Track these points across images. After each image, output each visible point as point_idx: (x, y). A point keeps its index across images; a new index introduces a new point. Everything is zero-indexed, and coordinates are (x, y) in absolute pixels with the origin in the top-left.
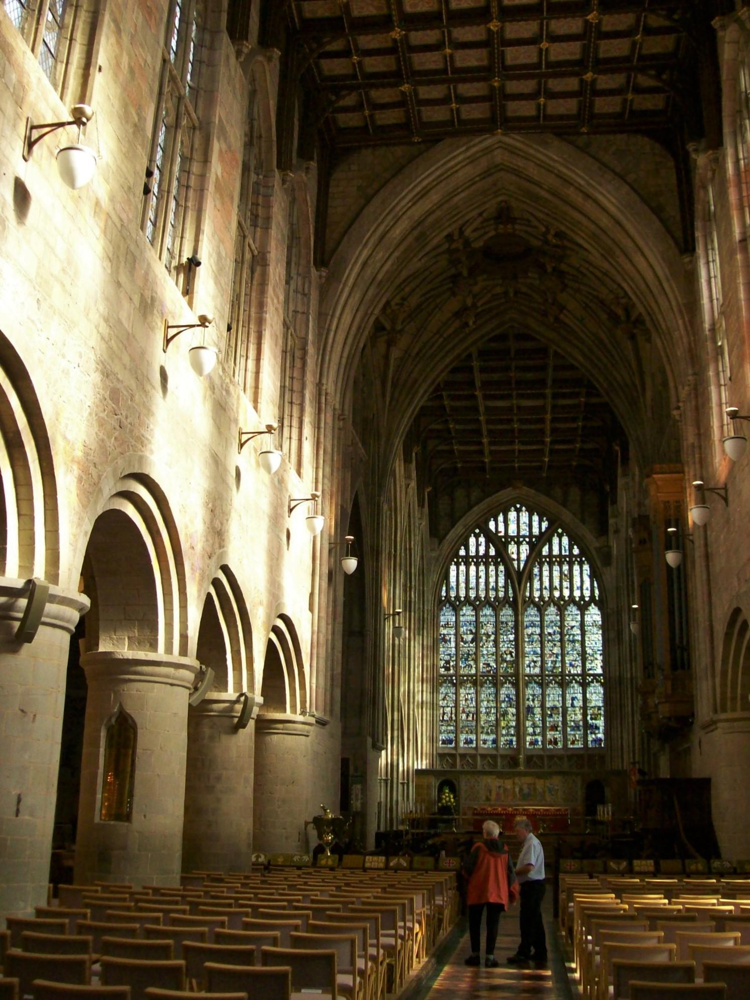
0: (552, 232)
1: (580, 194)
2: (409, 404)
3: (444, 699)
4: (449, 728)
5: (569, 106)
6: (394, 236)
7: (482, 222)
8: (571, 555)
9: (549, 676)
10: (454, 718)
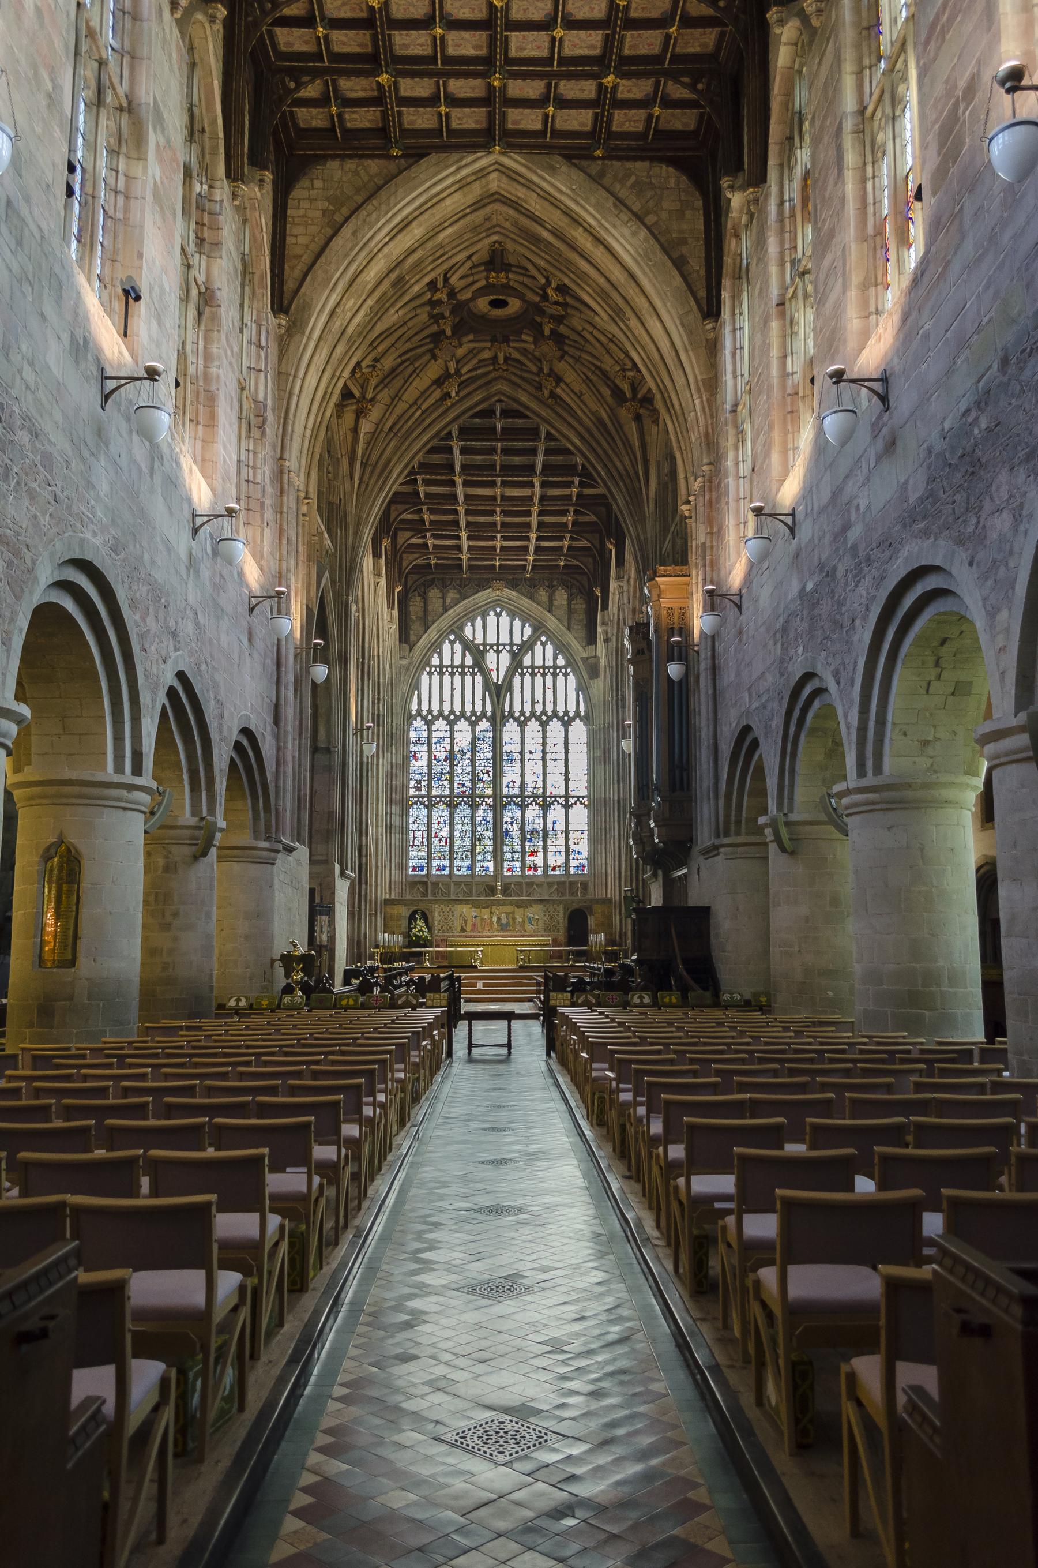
0: (554, 285)
1: (590, 238)
2: (381, 489)
4: (420, 854)
5: (580, 120)
6: (368, 278)
7: (471, 268)
8: (555, 667)
9: (529, 797)
10: (425, 843)
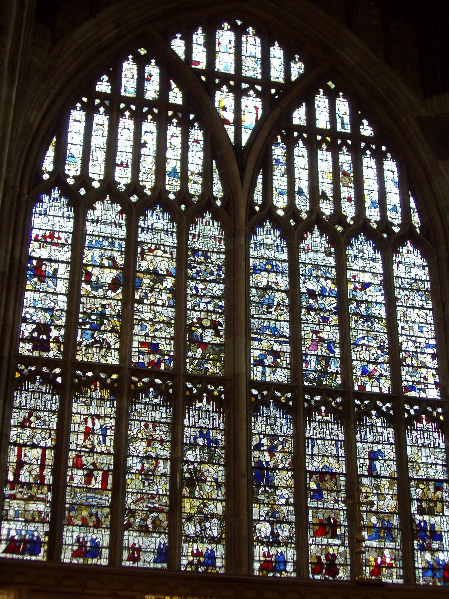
3: (22, 425)
4: (32, 506)
9: (312, 391)
10: (49, 480)
